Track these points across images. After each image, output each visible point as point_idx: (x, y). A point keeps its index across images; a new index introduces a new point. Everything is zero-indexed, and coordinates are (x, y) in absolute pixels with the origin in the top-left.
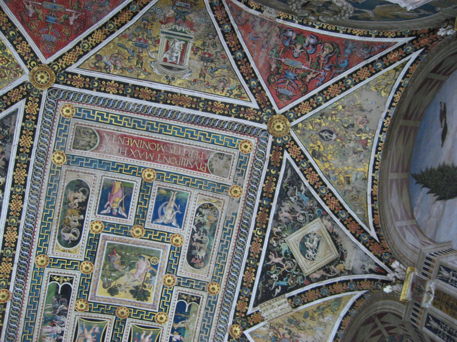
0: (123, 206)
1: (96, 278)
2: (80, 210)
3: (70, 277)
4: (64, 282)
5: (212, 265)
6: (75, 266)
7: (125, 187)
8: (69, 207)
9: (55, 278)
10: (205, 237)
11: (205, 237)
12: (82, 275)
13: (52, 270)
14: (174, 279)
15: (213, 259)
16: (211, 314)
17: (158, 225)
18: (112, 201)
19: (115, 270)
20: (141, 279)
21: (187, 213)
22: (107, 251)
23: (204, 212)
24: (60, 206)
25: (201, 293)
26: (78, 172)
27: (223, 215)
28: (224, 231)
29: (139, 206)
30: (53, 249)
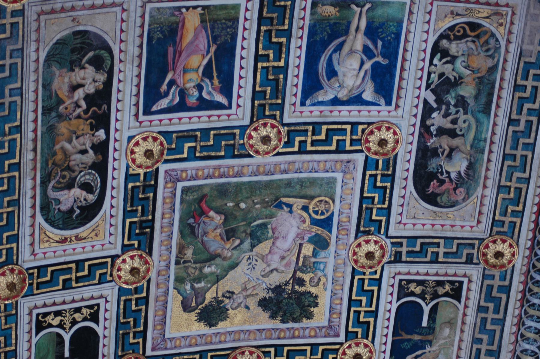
0: (215, 74)
1: (161, 291)
2: (95, 116)
3: (90, 307)
4: (74, 322)
5: (488, 192)
6: (99, 272)
7: (214, 21)
8: (60, 117)
9: (50, 319)
10: (462, 117)
11: (462, 117)
12: (121, 292)
13: (39, 300)
14: (382, 247)
15: (491, 174)
16: (494, 322)
17: (322, 108)
18: (180, 68)
19: (212, 258)
20: (288, 265)
21: (404, 60)
22: (181, 209)
23: (454, 48)
24: (35, 121)
25: (461, 269)
26: (73, 9)
27: (512, 48)
28: (518, 95)
29: (260, 65)
30: (32, 244)
